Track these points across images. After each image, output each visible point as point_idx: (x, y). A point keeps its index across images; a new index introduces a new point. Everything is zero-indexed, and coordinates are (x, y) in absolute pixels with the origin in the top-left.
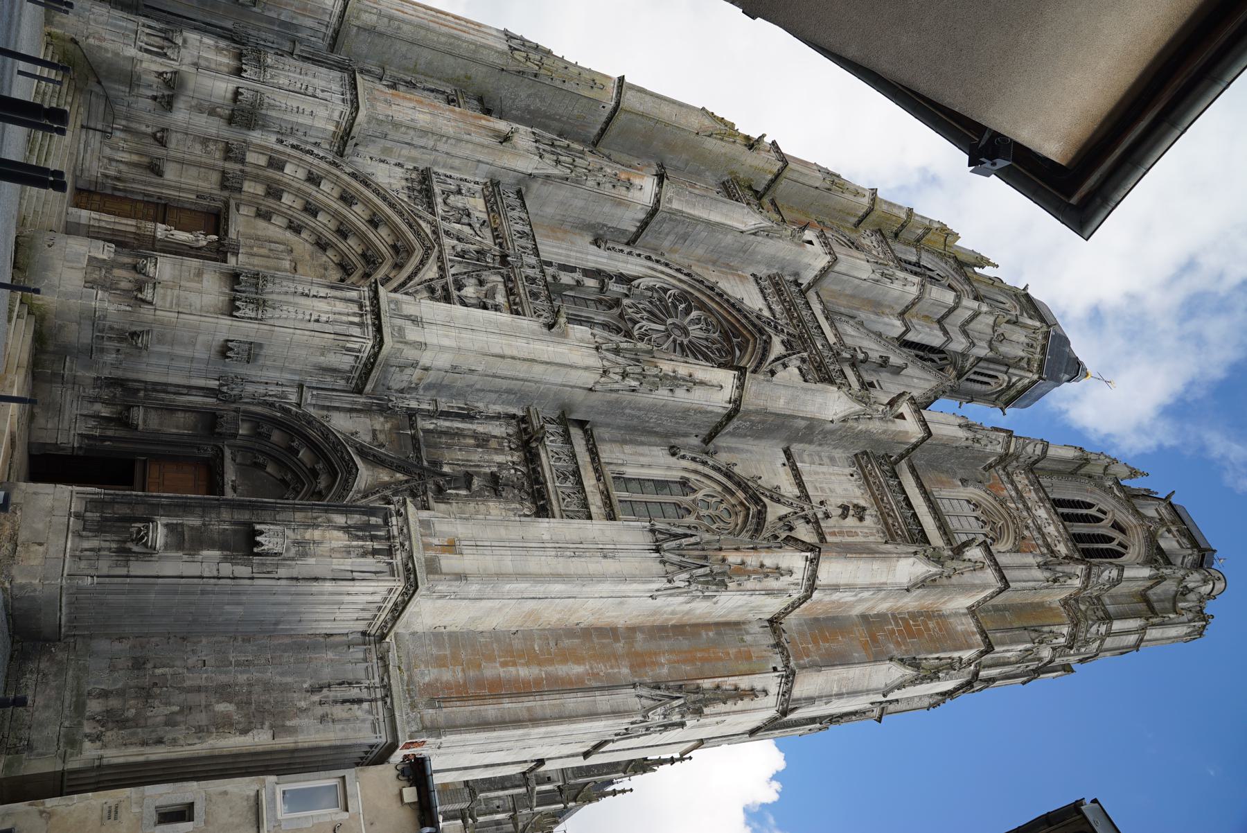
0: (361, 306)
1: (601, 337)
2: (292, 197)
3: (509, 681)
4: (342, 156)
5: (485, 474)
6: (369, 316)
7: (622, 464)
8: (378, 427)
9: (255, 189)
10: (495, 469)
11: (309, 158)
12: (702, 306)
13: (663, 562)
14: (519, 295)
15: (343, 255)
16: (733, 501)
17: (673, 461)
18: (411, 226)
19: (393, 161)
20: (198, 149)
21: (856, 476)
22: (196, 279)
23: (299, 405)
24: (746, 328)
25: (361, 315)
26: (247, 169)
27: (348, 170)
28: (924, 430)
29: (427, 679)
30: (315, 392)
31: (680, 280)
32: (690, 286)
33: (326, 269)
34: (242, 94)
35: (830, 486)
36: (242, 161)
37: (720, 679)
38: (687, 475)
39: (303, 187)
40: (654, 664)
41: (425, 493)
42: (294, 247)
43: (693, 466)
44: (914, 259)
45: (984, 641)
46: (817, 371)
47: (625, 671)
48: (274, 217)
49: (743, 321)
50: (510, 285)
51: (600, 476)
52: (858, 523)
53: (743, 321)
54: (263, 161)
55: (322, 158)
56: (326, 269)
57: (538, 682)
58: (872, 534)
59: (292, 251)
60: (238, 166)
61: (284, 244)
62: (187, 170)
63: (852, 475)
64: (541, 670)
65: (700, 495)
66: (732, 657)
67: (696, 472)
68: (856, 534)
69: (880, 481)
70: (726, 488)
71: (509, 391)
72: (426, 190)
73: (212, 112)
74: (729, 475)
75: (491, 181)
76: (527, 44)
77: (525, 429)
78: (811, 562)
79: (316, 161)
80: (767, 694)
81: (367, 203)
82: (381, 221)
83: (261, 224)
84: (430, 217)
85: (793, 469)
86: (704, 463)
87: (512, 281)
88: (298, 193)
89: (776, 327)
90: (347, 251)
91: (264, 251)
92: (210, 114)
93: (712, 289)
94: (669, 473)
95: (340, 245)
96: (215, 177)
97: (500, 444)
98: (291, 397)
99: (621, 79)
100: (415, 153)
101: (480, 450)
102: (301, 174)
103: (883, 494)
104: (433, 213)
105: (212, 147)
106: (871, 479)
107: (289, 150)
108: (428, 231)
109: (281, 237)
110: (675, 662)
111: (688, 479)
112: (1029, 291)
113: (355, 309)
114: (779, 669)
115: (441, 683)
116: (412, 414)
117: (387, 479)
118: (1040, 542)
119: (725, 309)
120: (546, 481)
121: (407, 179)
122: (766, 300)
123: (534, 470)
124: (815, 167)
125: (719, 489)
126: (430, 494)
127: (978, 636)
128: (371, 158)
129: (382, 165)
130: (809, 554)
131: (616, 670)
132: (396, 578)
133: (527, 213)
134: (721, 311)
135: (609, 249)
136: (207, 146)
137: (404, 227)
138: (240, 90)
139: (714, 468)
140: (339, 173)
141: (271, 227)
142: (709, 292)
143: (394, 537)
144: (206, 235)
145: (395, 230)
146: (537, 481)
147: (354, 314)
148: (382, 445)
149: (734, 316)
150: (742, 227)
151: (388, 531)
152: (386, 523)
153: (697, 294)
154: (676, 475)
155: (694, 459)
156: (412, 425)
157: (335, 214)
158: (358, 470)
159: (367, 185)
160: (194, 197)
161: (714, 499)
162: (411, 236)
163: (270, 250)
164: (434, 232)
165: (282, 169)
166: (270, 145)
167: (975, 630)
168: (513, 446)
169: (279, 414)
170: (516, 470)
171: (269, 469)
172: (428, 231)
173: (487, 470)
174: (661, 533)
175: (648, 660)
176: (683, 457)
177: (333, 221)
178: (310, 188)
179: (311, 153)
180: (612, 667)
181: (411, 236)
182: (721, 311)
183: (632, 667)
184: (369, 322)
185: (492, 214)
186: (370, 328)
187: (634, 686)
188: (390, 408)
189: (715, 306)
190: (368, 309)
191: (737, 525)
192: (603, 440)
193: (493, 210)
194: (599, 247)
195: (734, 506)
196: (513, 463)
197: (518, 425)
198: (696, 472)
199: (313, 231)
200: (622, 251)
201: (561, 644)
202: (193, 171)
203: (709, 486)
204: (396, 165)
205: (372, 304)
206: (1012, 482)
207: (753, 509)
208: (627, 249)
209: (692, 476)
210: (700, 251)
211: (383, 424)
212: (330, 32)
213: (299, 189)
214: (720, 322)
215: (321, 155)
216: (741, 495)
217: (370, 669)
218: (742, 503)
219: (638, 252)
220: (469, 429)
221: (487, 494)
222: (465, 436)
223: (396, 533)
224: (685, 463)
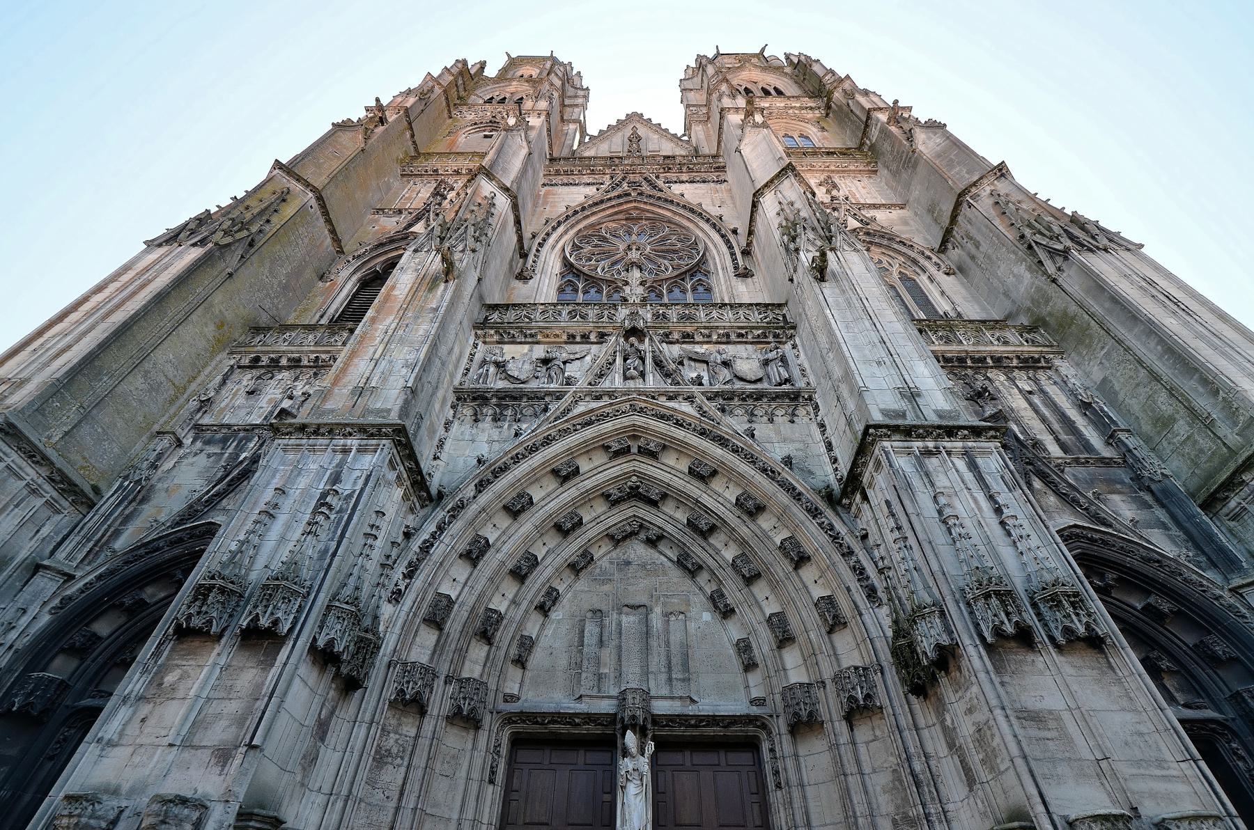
0: (928, 453)
4: (441, 495)
9: (476, 662)
11: (438, 551)
18: (589, 423)
19: (441, 432)
20: (392, 776)
22: (1052, 724)
26: (444, 669)
27: (470, 491)
31: (566, 232)
32: (572, 226)
34: (331, 643)
36: (429, 673)
39: (488, 573)
42: (587, 606)
48: (526, 634)
50: (676, 336)
54: (428, 637)
55: (441, 528)
56: (628, 563)
59: (597, 612)
60: (439, 684)
61: (583, 621)
62: (436, 805)
73: (322, 729)
75: (474, 328)
76: (192, 226)
79: (446, 538)
81: (534, 477)
83: (537, 658)
84: (568, 399)
87: (670, 333)
90: (601, 527)
91: (608, 655)
92: (322, 739)
95: (591, 534)
96: (455, 739)
99: (278, 164)
102: (461, 571)
104: (559, 396)
105: (391, 742)
107: (418, 583)
108: (594, 405)
109: (565, 627)
112: (513, 56)
113: (932, 463)
121: (476, 421)
128: (436, 458)
129: (446, 447)
134: (608, 212)
136: (389, 751)
138: (321, 643)
140: (473, 508)
141: (543, 642)
142: (579, 216)
144: (626, 753)
145: (587, 449)
146: (961, 360)
150: (524, 151)
153: (581, 226)
157: (540, 531)
159: (504, 469)
160: (491, 787)
162: (608, 426)
163: (601, 643)
165: (450, 602)
166: (403, 615)
172: (594, 405)
177: (546, 539)
178: (491, 562)
179: (426, 548)
181: (608, 426)
182: (608, 212)
185: (539, 337)
186: (970, 444)
193: (532, 336)
194: (531, 278)
202: (440, 788)
204: (447, 430)
205: (921, 437)
208: (531, 258)
212: (50, 492)
213: (491, 580)
215: (433, 528)
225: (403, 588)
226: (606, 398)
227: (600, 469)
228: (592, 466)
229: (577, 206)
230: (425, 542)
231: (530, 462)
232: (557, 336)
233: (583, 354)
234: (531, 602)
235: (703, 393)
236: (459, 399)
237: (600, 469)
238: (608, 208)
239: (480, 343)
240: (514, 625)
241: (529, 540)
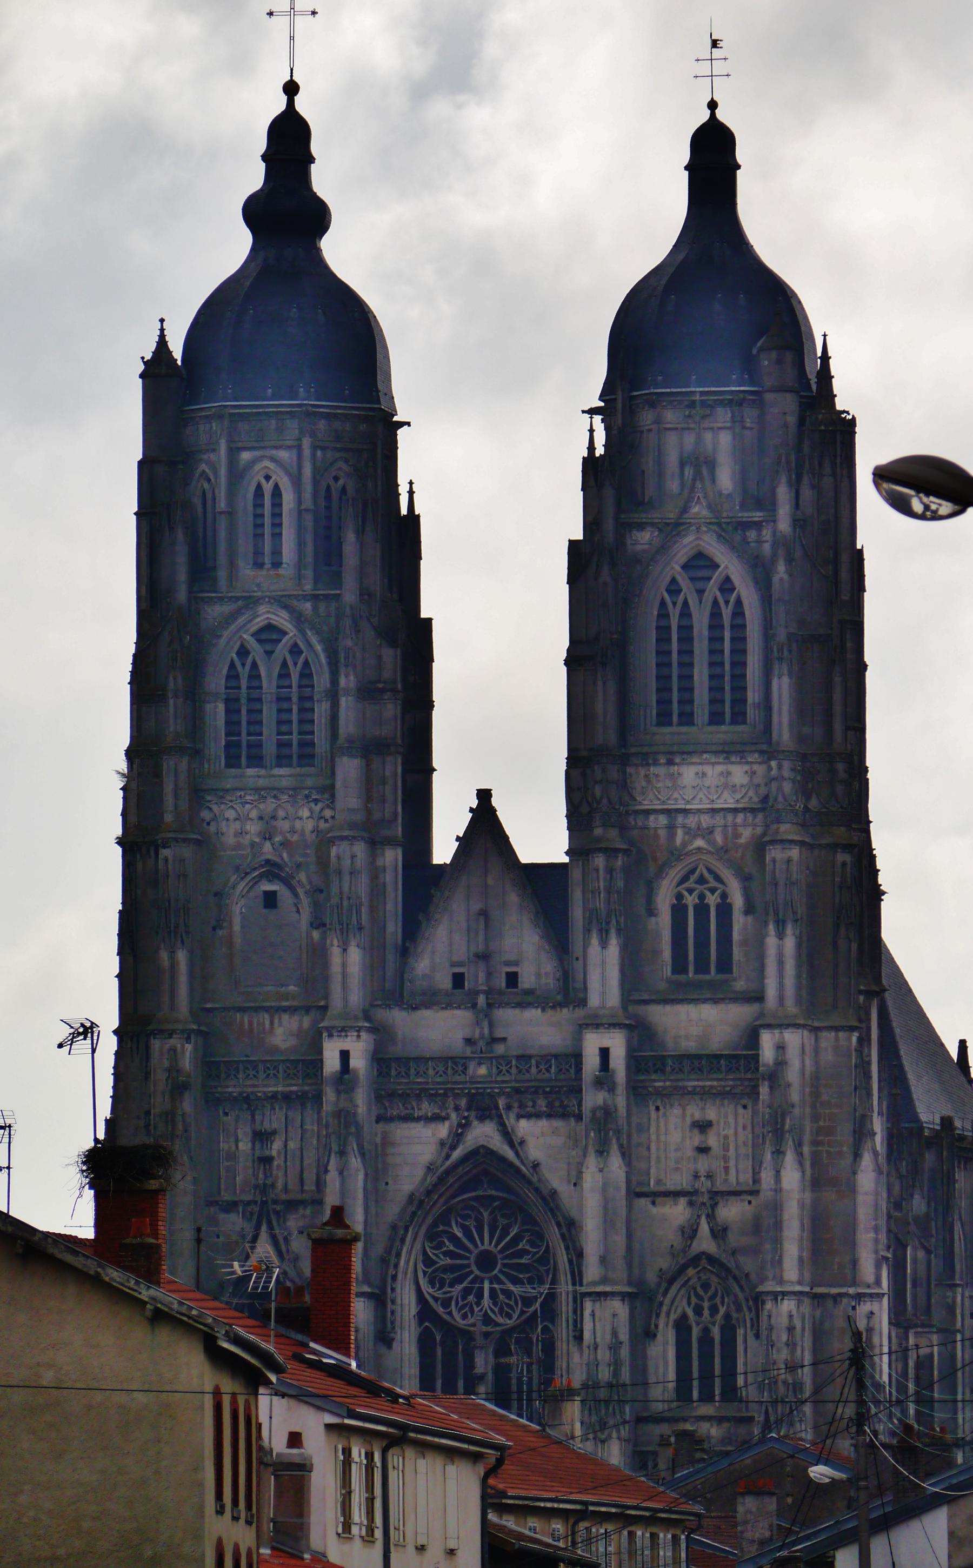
17: (660, 1337)
21: (659, 1103)
28: (620, 1028)
38: (671, 1323)
43: (663, 1315)
44: (221, 707)
45: (845, 1031)
52: (715, 1128)
58: (726, 1116)
63: (657, 1109)
65: (690, 1312)
68: (726, 1137)
70: (683, 1285)
74: (671, 1282)
80: (872, 1313)
85: (659, 1196)
86: (661, 1304)
93: (421, 1203)
103: (685, 1088)
114: (853, 1304)
118: (730, 817)
119: (447, 1189)
125: (683, 1291)
130: (779, 1298)
135: (394, 1328)
150: (361, 1177)
153: (429, 1220)
155: (658, 1315)
167: (833, 1034)
176: (657, 1326)
189: (442, 1200)
194: (393, 1339)
200: (393, 1312)
206: (648, 812)
207: (704, 1263)
209: (673, 1317)
216: (691, 1272)
218: (698, 1272)
219: (389, 1291)
224: (661, 1326)
238: (455, 1182)
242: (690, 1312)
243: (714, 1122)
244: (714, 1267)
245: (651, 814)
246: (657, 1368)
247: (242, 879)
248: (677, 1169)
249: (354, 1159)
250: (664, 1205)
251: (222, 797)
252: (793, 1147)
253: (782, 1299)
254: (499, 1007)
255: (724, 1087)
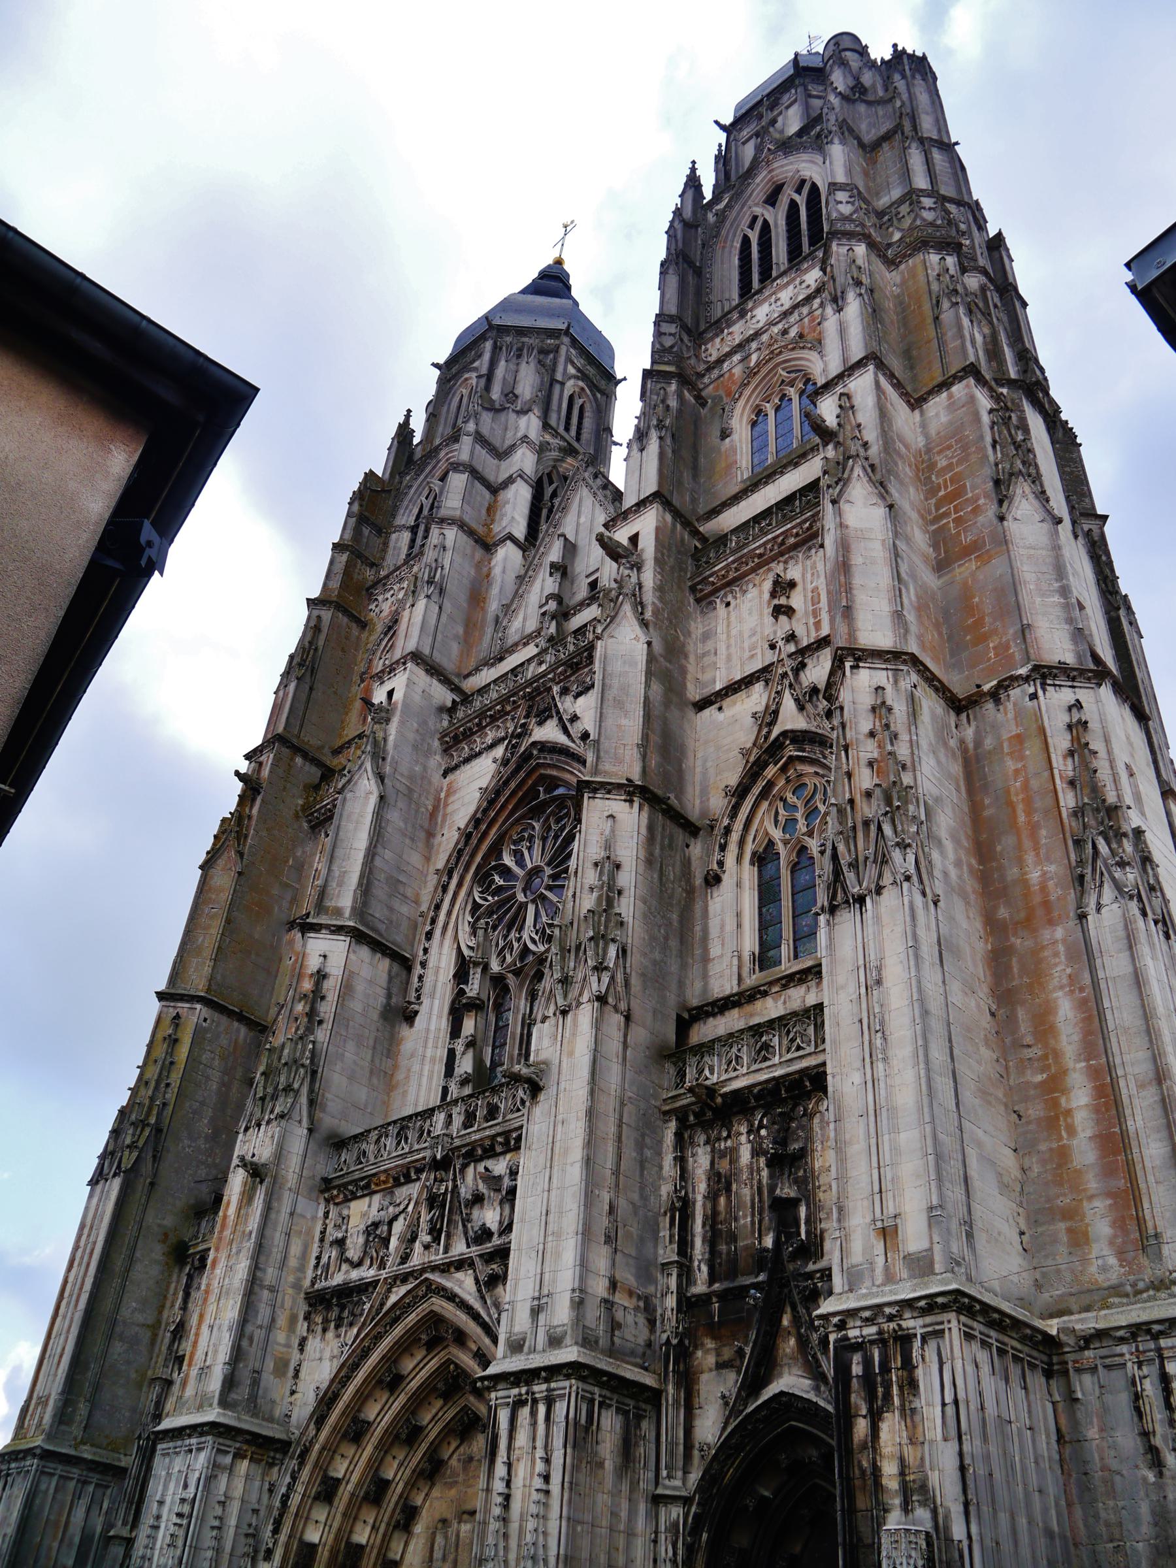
1: (547, 1007)
2: (359, 1526)
3: (1098, 1122)
5: (771, 1176)
6: (536, 1388)
7: (739, 958)
8: (711, 1360)
10: (762, 1160)
12: (495, 850)
13: (879, 890)
14: (493, 1137)
15: (448, 1432)
16: (781, 782)
17: (728, 880)
18: (396, 1320)
19: (295, 1356)
23: (686, 1501)
24: (523, 781)
25: (535, 1401)
27: (312, 1430)
29: (1112, 1261)
30: (664, 1473)
31: (460, 885)
32: (467, 869)
33: (471, 1459)
35: (746, 635)
37: (1058, 781)
39: (341, 1508)
40: (1043, 889)
41: (810, 1276)
42: (437, 1517)
43: (733, 849)
44: (406, 536)
45: (961, 379)
46: (578, 669)
47: (1059, 933)
49: (513, 785)
51: (760, 992)
52: (799, 588)
53: (513, 785)
55: (294, 1478)
57: (1094, 1074)
58: (814, 567)
59: (444, 1521)
61: (434, 1535)
63: (728, 604)
64: (1074, 1069)
65: (777, 834)
66: (1019, 766)
67: (742, 843)
68: (815, 590)
69: (733, 562)
70: (764, 794)
71: (640, 1146)
72: (339, 1298)
75: (322, 1192)
76: (110, 1148)
77: (696, 1115)
78: (858, 659)
81: (362, 1397)
82: (389, 1370)
85: (727, 695)
86: (728, 830)
87: (474, 1149)
88: (351, 1516)
89: (519, 736)
93: (469, 836)
94: (746, 883)
97: (723, 1155)
98: (674, 1515)
99: (161, 996)
100: (282, 1320)
101: (734, 1187)
102: (320, 1513)
103: (752, 555)
104: (374, 1283)
106: (732, 575)
107: (283, 1538)
108: (402, 1290)
110: (1038, 855)
111: (754, 854)
112: (441, 361)
114: (1032, 690)
115: (1115, 1236)
116: (688, 1304)
117: (792, 1342)
118: (805, 310)
120: (774, 1078)
121: (325, 1330)
122: (480, 754)
123: (758, 1097)
124: (281, 693)
125: (765, 805)
126: (811, 1267)
127: (954, 389)
128: (293, 1393)
129: (302, 1375)
130: (848, 665)
131: (1061, 948)
132: (946, 1326)
133: (369, 1131)
135: (418, 998)
137: (398, 1331)
139: (734, 814)
140: (317, 1447)
142: (474, 841)
143: (880, 1332)
145: (404, 1347)
147: (534, 1414)
148: (740, 1353)
149: (507, 801)
150: (373, 800)
151: (872, 1342)
152: (858, 1347)
153: (478, 859)
154: (749, 874)
155: (723, 848)
156: (705, 1299)
157: (385, 1448)
158: (782, 1393)
161: (781, 811)
162: (412, 1318)
163: (444, 1559)
164: (404, 1278)
165: (313, 1547)
167: (944, 395)
168: (725, 1134)
169: (705, 1536)
170: (761, 1126)
171: (797, 1549)
172: (402, 1290)
173: (765, 1173)
174: (834, 897)
175: (1037, 899)
176: (721, 864)
177: (394, 1451)
180: (1056, 954)
181: (412, 1318)
182: (501, 821)
183: (1051, 923)
184: (544, 1387)
186: (553, 1385)
187: (1082, 917)
188: (681, 1342)
190: (524, 1390)
191: (816, 773)
192: (705, 989)
193: (367, 1186)
194: (416, 1013)
195: (788, 781)
196: (749, 1133)
197: (692, 1127)
198: (742, 843)
199: (411, 1485)
200: (421, 977)
201: (1028, 1040)
203: (762, 821)
204: (302, 1350)
205: (516, 1384)
206: (720, 362)
207: (791, 751)
208: (418, 970)
209: (749, 848)
210: (415, 859)
211: (707, 1351)
212: (95, 1478)
213: (344, 1515)
214: (517, 820)
215: (288, 1479)
216: (771, 771)
217: (1108, 1361)
218: (784, 769)
219: (421, 953)
220: (704, 1205)
221: (801, 1173)
222: (715, 1213)
223: (873, 1330)
225: (271, 1545)
226: (411, 1279)
227: (421, 1365)
228: (415, 1362)
229: (467, 826)
230: (283, 1495)
231: (355, 1382)
232: (385, 1182)
233: (406, 1202)
234: (388, 1524)
235: (481, 1256)
236: (310, 1305)
237: (421, 1365)
239: (332, 1206)
240: (375, 1551)
241: (375, 1465)
242: (777, 834)
243: (797, 580)
244: (804, 751)
245: (724, 361)
246: (722, 927)
247: (386, 634)
248: (752, 656)
249: (366, 782)
250: (735, 703)
251: (385, 585)
252: (865, 479)
253: (855, 667)
254: (575, 614)
255: (800, 524)
